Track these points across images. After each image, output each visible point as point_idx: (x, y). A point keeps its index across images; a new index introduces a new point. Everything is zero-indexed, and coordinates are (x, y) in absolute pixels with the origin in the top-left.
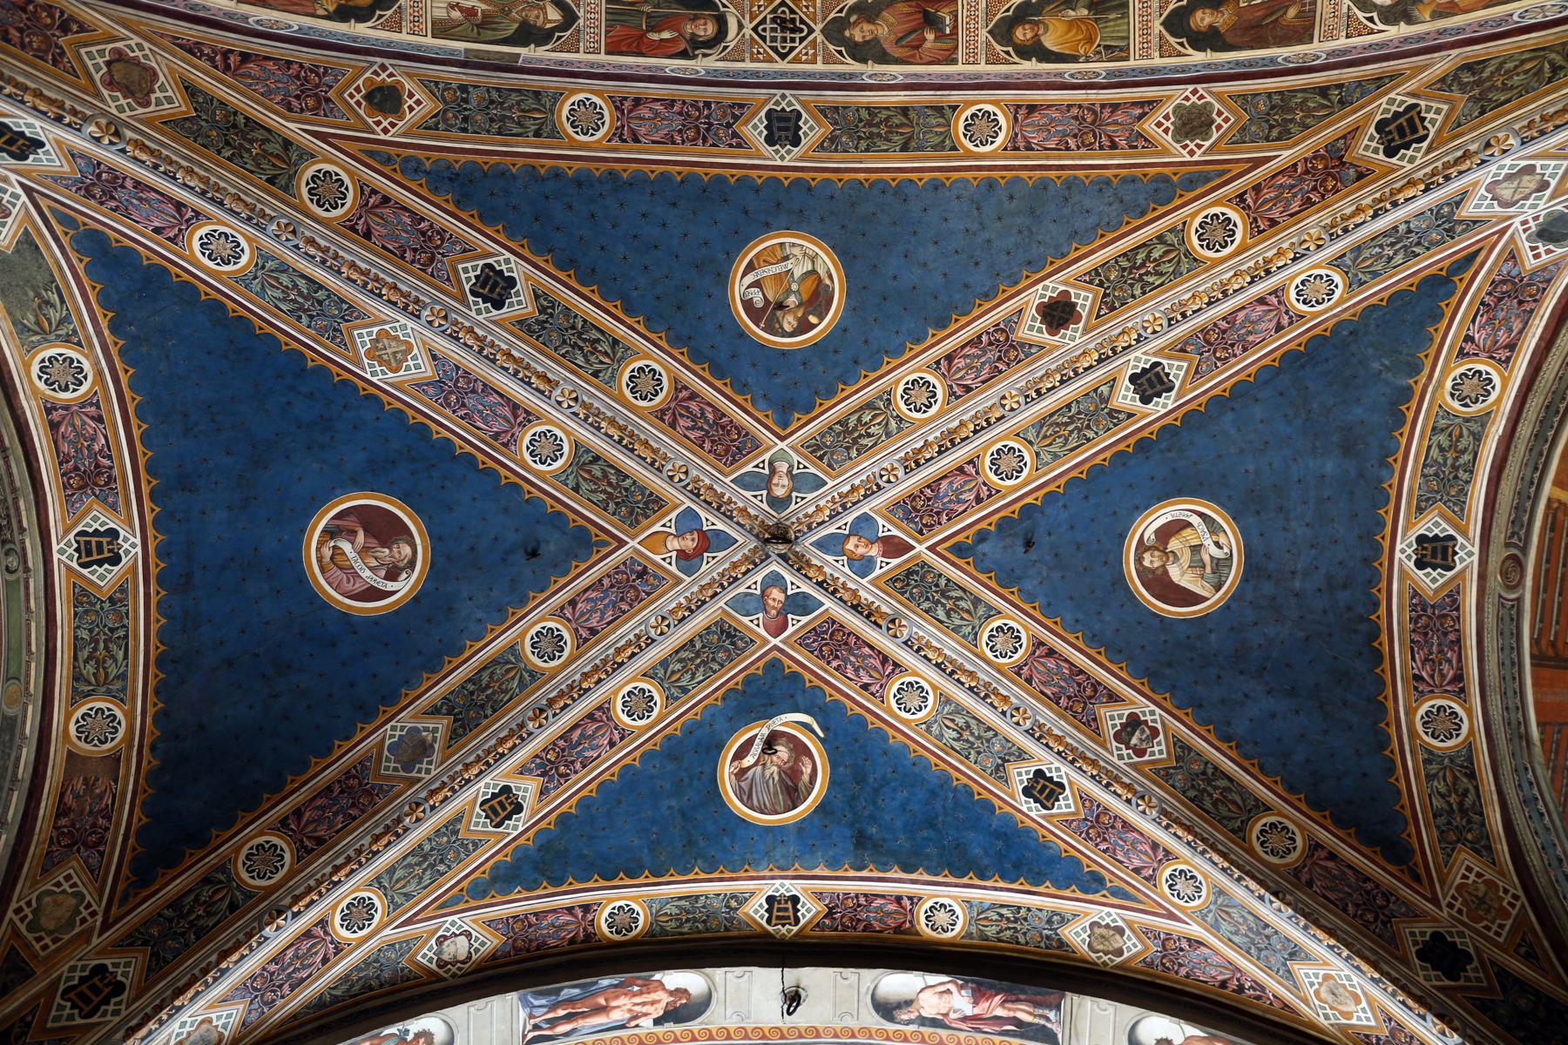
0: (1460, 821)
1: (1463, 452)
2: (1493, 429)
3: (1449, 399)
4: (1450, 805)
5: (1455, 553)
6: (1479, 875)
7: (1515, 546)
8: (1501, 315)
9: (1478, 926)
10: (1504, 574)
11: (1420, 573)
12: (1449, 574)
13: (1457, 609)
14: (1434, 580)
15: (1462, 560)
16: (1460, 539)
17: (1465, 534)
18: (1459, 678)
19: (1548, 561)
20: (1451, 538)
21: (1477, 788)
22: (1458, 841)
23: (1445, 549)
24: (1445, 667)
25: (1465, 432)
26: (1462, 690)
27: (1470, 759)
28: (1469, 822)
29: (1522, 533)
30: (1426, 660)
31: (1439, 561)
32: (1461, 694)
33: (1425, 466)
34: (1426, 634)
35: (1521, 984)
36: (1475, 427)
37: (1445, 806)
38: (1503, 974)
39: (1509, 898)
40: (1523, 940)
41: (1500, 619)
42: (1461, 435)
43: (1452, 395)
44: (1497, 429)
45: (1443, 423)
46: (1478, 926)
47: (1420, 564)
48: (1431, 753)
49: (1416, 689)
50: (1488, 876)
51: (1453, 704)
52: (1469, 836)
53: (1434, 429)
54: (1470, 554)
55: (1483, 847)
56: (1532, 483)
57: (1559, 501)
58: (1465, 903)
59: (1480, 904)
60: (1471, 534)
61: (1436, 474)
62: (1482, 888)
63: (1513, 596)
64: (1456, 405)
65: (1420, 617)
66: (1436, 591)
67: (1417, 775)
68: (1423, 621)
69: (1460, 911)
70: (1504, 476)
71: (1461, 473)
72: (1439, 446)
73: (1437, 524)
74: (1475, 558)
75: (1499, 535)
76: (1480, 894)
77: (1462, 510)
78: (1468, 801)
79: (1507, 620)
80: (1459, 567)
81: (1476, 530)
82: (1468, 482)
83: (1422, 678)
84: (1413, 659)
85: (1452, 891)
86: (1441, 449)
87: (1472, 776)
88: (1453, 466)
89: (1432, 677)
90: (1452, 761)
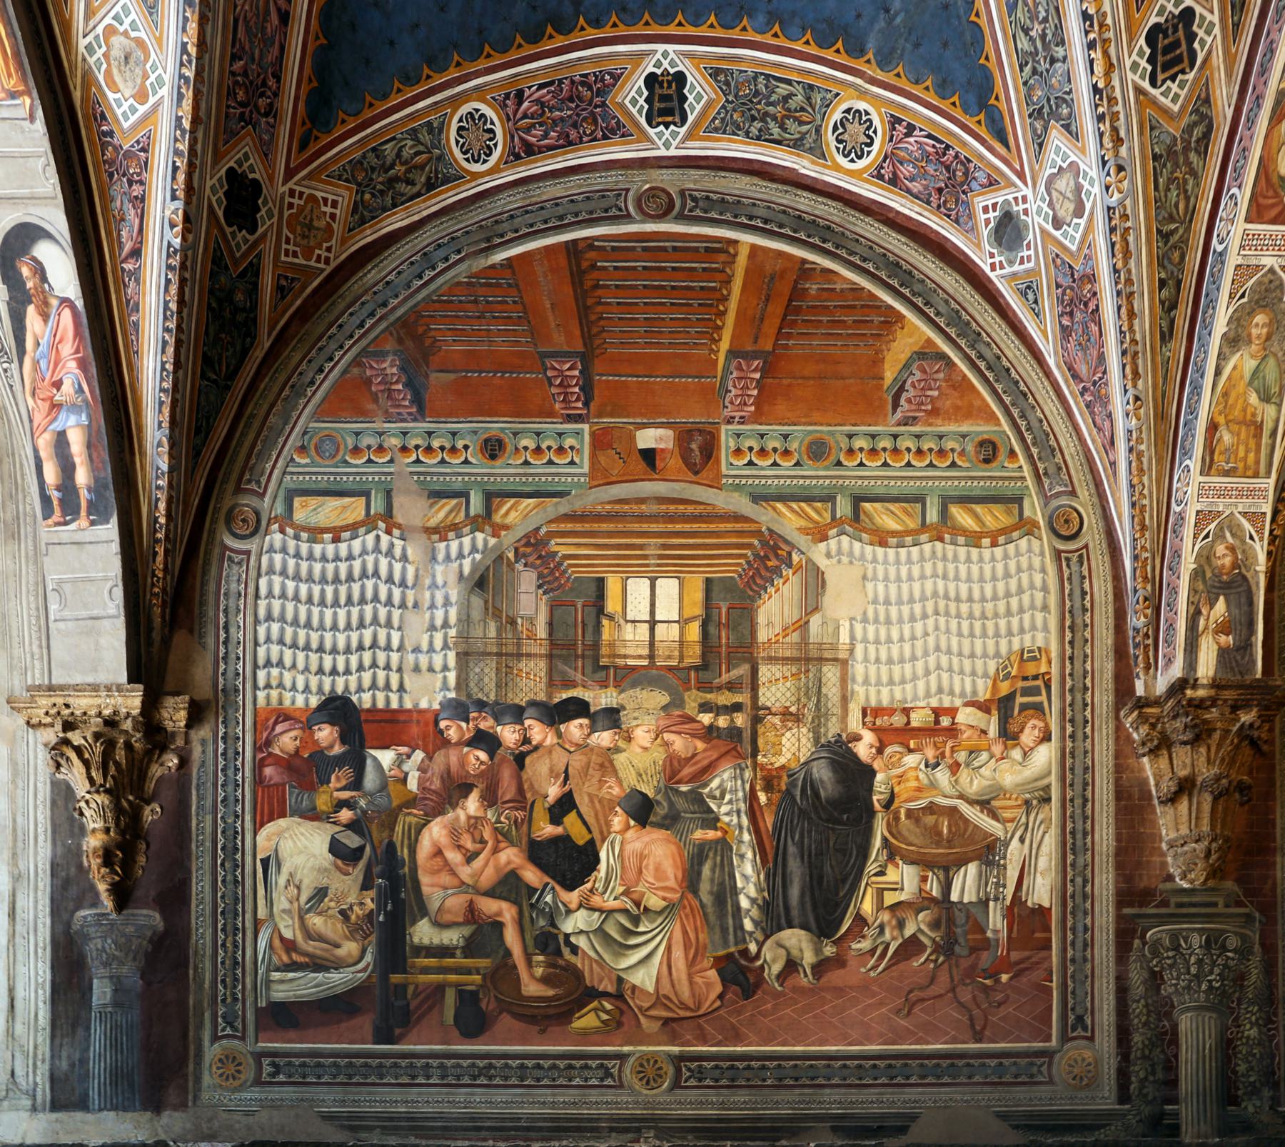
0: (382, 182)
1: (783, 127)
2: (806, 163)
3: (844, 106)
4: (392, 166)
5: (667, 126)
6: (333, 216)
7: (684, 205)
8: (930, 169)
9: (285, 231)
10: (654, 192)
11: (641, 82)
12: (643, 121)
13: (605, 137)
14: (634, 102)
15: (660, 135)
16: (683, 130)
17: (690, 136)
18: (531, 151)
19: (675, 248)
20: (684, 119)
21: (418, 195)
22: (359, 185)
23: (670, 112)
24: (538, 132)
25: (805, 128)
26: (518, 157)
27: (447, 180)
28: (381, 192)
29: (698, 212)
30: (543, 105)
31: (657, 105)
32: (513, 157)
33: (767, 76)
34: (571, 100)
35: (254, 290)
36: (809, 141)
37: (389, 160)
38: (254, 270)
39: (324, 254)
40: (293, 280)
41: (603, 194)
42: (801, 123)
43: (848, 111)
44: (804, 166)
45: (817, 98)
46: (285, 231)
47: (651, 80)
48: (441, 130)
49: (507, 96)
50: (335, 226)
51: (500, 147)
52: (367, 196)
53: (811, 87)
54: (667, 145)
55: (362, 215)
56: (751, 218)
57: (736, 255)
58: (301, 209)
59: (306, 225)
60: (689, 144)
61: (757, 93)
62: (322, 224)
63: (631, 208)
64: (837, 116)
65: (590, 88)
66: (622, 106)
67: (412, 117)
68: (586, 94)
69: (291, 206)
70: (756, 180)
71: (757, 124)
72: (791, 95)
73: (698, 98)
74: (663, 152)
75: (693, 180)
76: (316, 223)
77: (716, 130)
78: (402, 187)
79: (604, 204)
80: (652, 132)
81: (696, 149)
82: (747, 134)
83: (520, 103)
84: (541, 87)
85: (307, 191)
86: (786, 99)
87: (430, 186)
88: (766, 114)
89: (525, 116)
90: (440, 158)
